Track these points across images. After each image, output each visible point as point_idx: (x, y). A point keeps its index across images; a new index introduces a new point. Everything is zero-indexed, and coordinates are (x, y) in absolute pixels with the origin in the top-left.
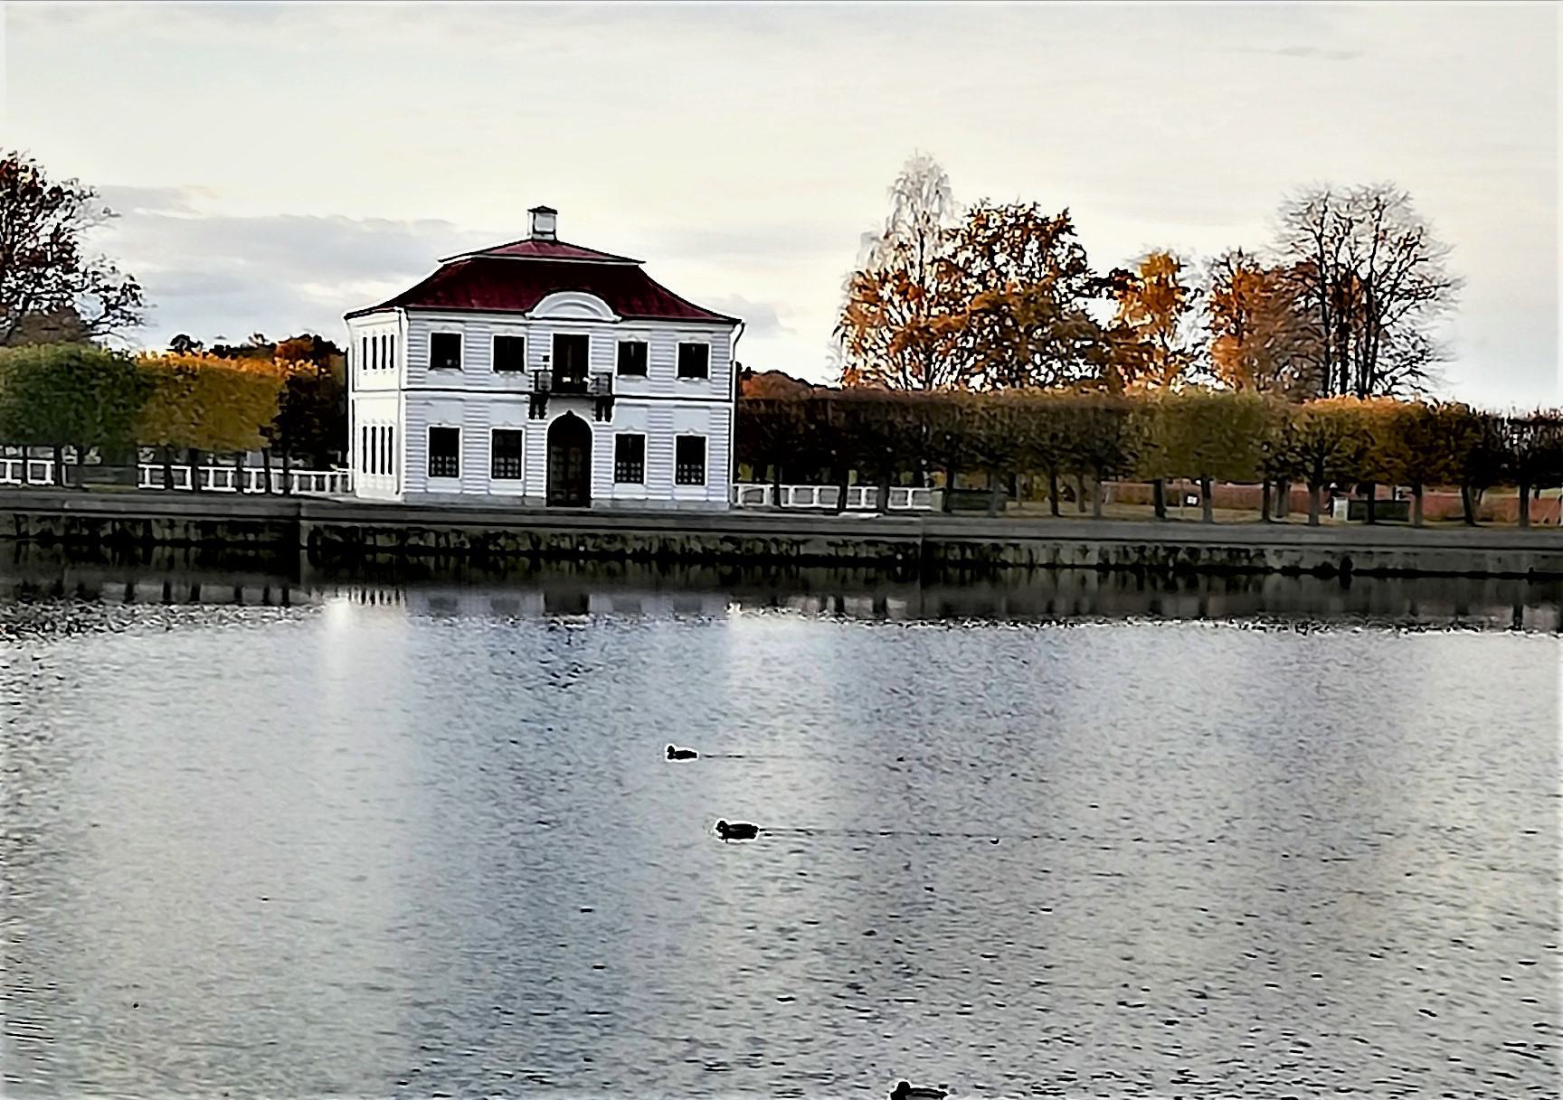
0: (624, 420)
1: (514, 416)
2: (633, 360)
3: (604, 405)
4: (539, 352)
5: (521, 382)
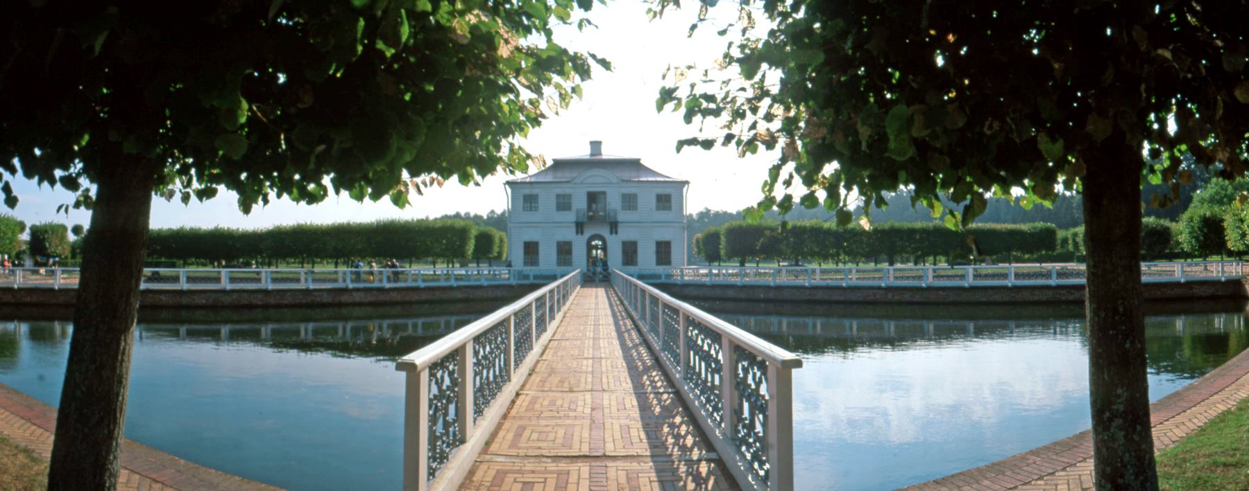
0: (625, 234)
1: (569, 234)
2: (630, 201)
3: (614, 226)
4: (580, 203)
5: (570, 217)
